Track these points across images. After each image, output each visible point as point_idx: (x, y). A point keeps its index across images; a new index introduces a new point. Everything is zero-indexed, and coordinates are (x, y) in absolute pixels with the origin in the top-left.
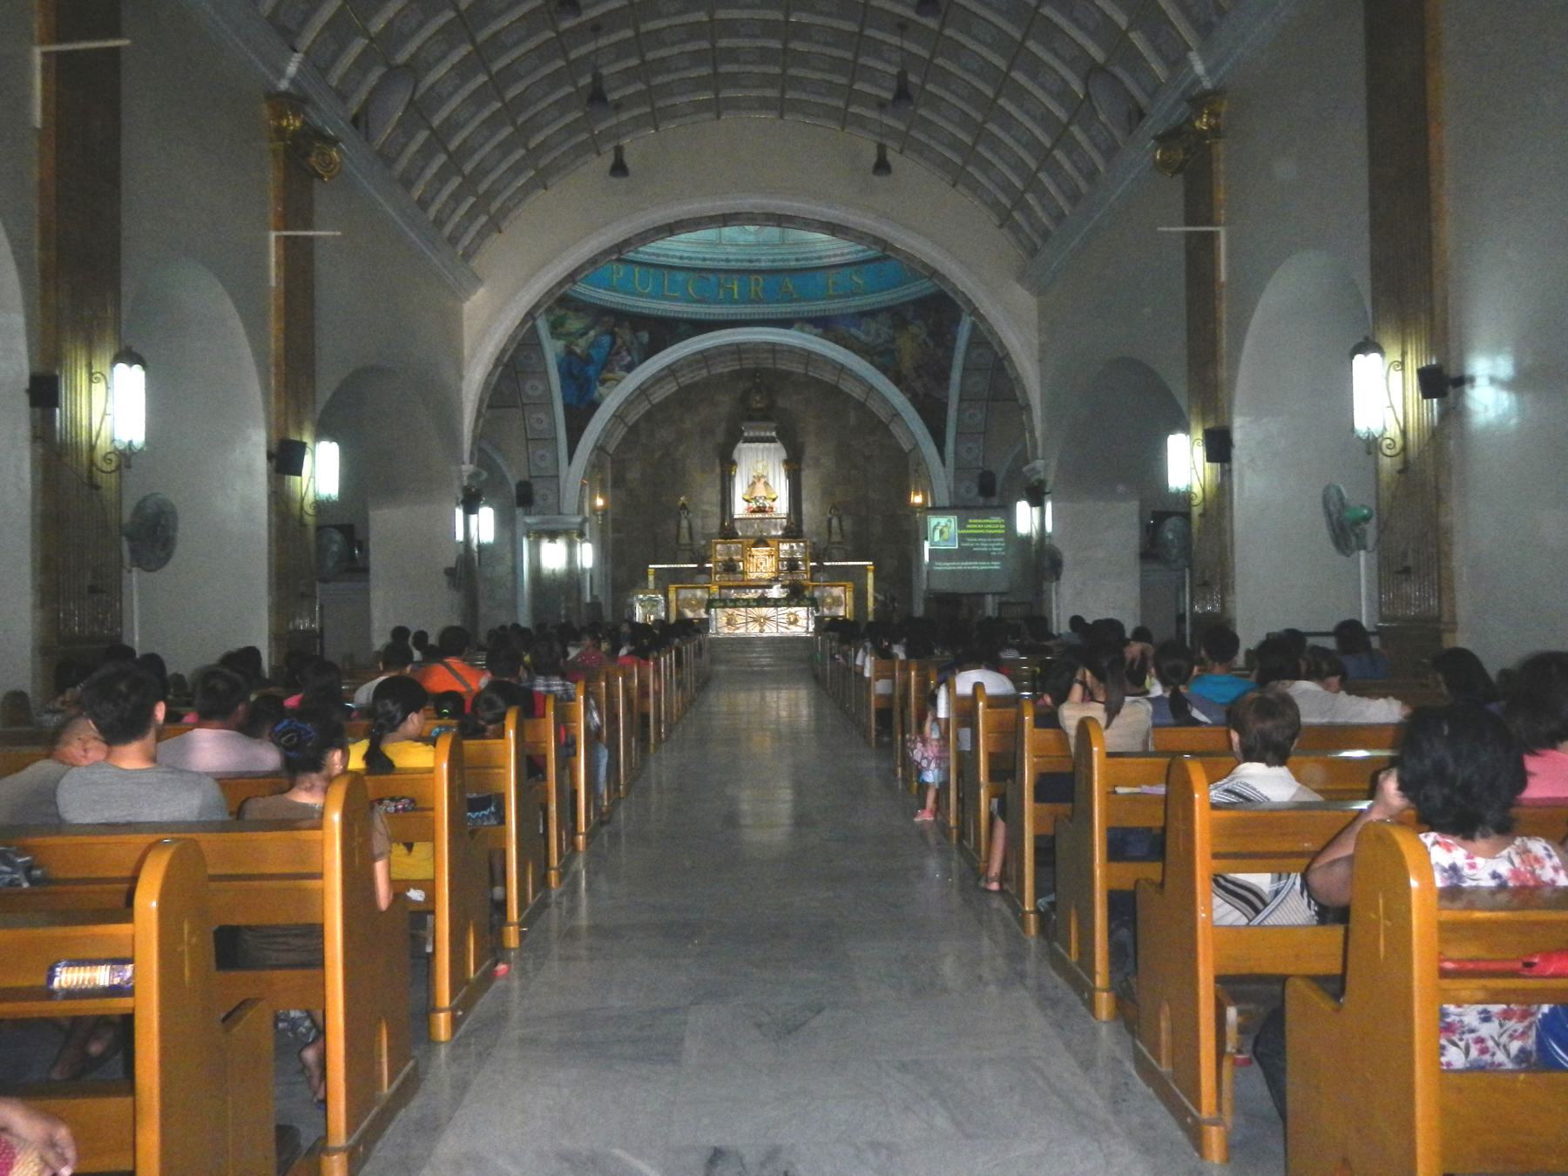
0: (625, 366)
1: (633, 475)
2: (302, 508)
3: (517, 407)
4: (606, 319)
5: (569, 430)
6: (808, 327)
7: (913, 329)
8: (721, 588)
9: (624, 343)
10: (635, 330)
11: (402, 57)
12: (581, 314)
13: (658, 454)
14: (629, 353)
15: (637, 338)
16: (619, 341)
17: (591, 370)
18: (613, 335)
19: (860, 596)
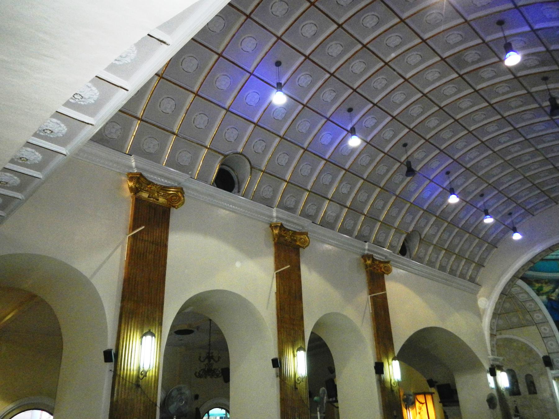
2: (391, 385)
11: (411, 229)
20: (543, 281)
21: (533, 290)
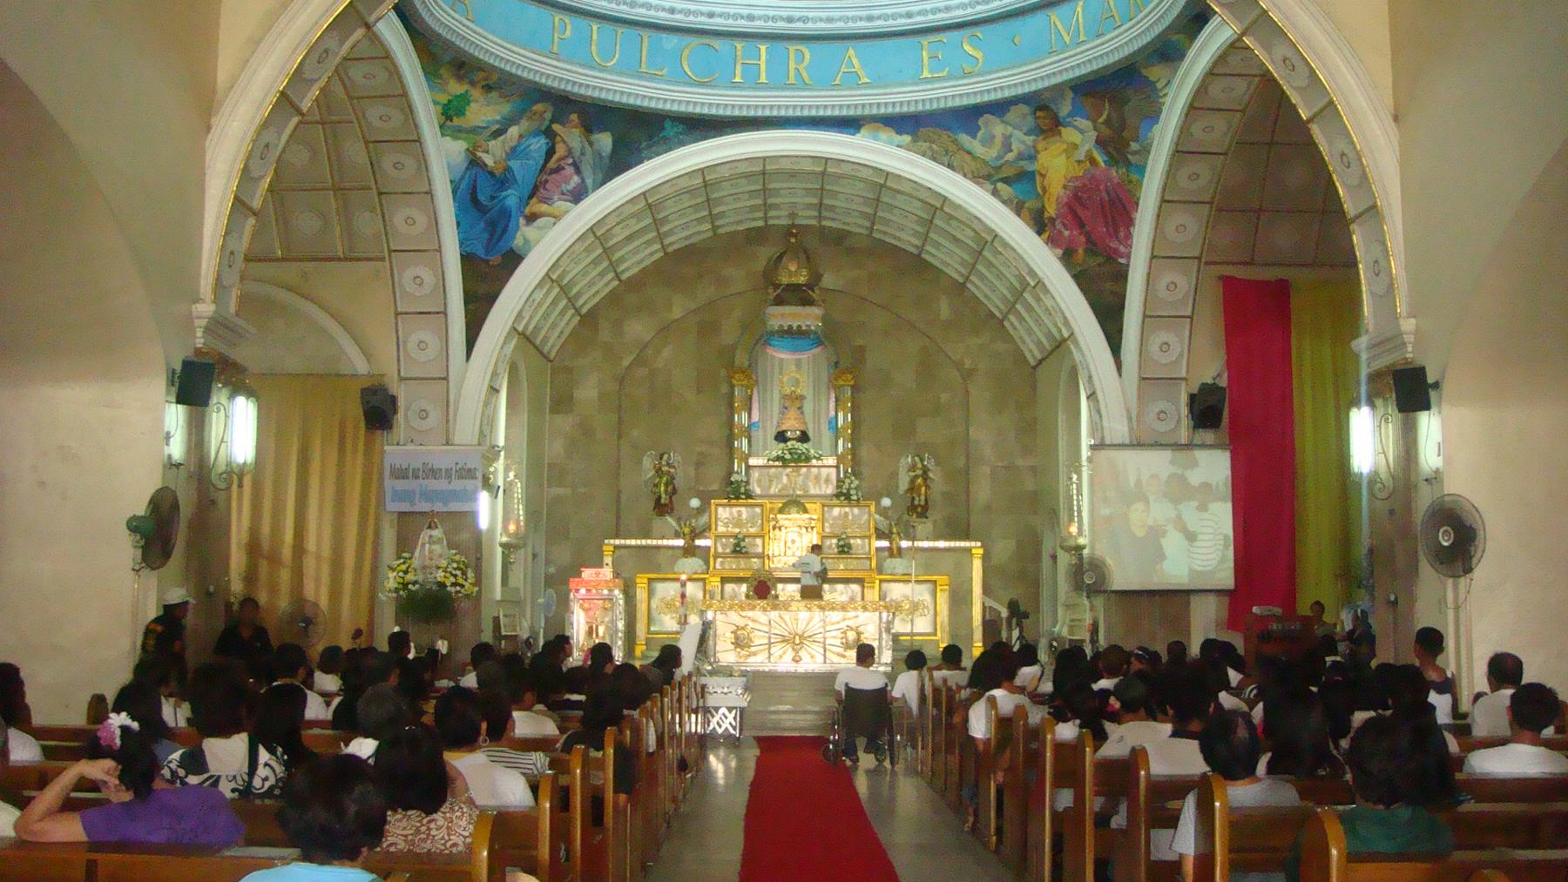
0: (571, 192)
1: (588, 392)
3: (383, 259)
4: (539, 107)
5: (469, 298)
6: (887, 134)
7: (1070, 135)
8: (724, 580)
9: (570, 152)
10: (588, 129)
12: (494, 94)
13: (626, 363)
14: (578, 171)
15: (591, 144)
16: (560, 150)
17: (511, 198)
18: (550, 134)
19: (959, 599)
20: (481, 75)
21: (435, 103)
